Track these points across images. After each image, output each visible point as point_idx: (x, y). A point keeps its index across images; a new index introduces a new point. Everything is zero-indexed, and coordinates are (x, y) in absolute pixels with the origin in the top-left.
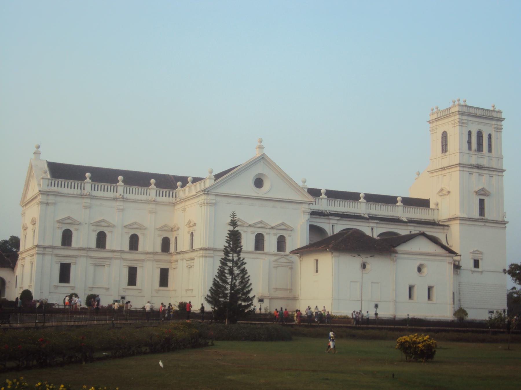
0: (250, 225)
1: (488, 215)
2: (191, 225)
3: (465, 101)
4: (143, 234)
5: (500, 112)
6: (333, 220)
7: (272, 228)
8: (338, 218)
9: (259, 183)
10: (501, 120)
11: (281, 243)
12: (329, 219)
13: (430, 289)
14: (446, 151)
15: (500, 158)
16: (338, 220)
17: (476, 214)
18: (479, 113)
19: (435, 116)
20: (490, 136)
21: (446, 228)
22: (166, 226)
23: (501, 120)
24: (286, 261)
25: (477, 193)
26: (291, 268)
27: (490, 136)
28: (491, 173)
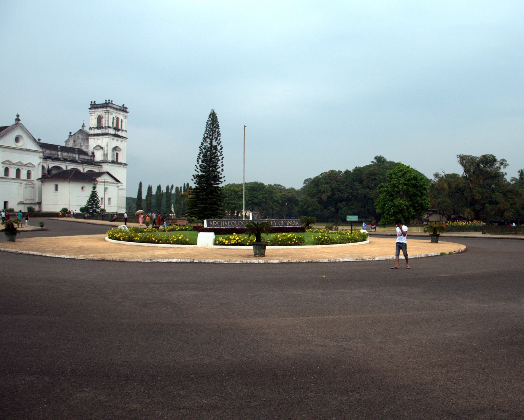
0: (14, 164)
1: (119, 161)
3: (112, 101)
5: (126, 108)
7: (25, 165)
9: (17, 140)
11: (29, 174)
12: (47, 161)
13: (109, 199)
16: (51, 161)
17: (115, 160)
18: (118, 107)
20: (122, 120)
21: (100, 167)
24: (31, 184)
26: (34, 188)
27: (122, 120)
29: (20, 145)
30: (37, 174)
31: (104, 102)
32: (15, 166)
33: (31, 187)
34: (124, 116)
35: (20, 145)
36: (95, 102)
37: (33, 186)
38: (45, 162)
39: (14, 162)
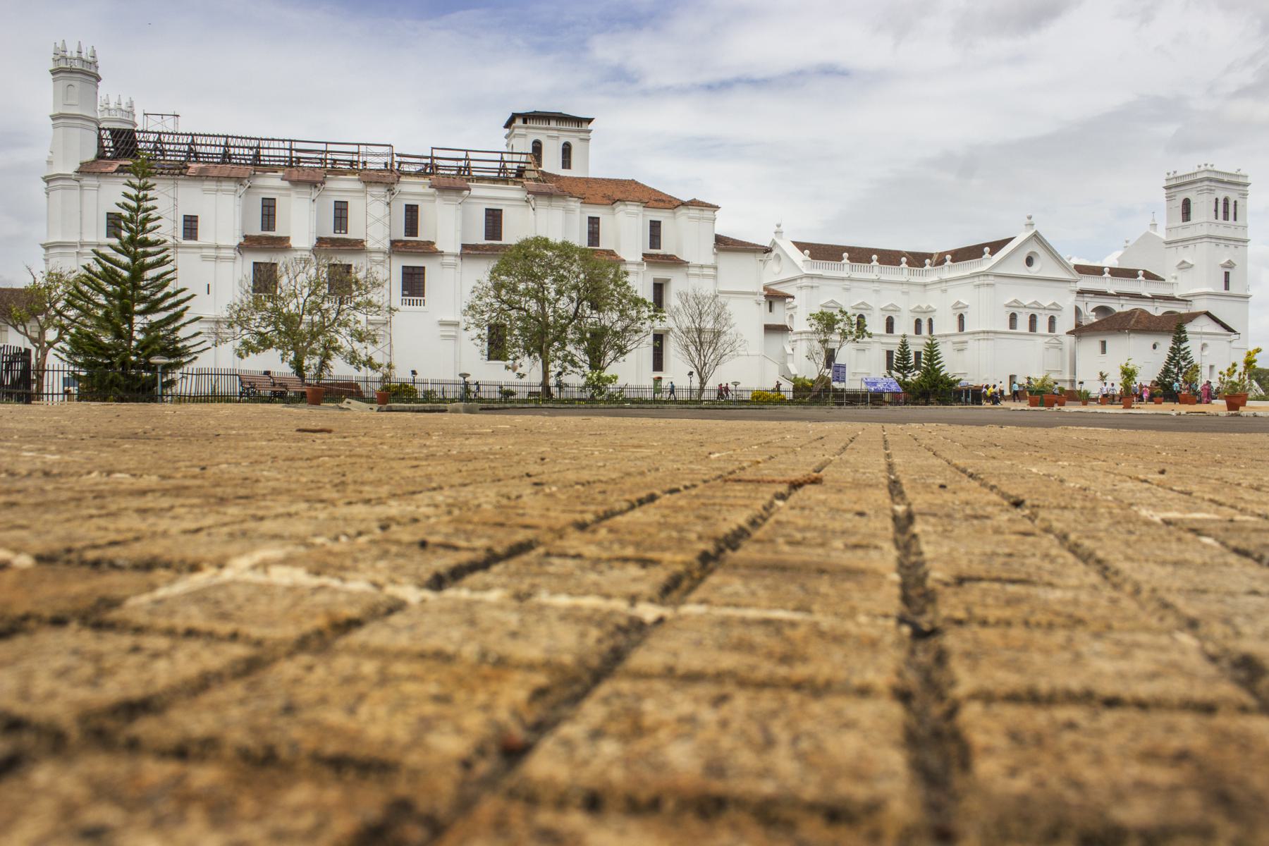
0: (1025, 307)
2: (957, 306)
3: (1212, 166)
4: (898, 316)
6: (1087, 298)
7: (1045, 308)
8: (1092, 295)
9: (1029, 261)
10: (1246, 185)
14: (1188, 219)
15: (1245, 227)
19: (1173, 182)
20: (1235, 202)
22: (919, 307)
23: (1246, 185)
25: (1223, 266)
27: (1235, 202)
28: (1236, 243)
29: (1035, 270)
30: (1066, 322)
31: (1196, 169)
32: (1027, 310)
33: (1057, 348)
34: (1240, 194)
35: (1035, 270)
36: (1175, 172)
37: (1059, 346)
38: (1081, 299)
39: (1026, 304)
